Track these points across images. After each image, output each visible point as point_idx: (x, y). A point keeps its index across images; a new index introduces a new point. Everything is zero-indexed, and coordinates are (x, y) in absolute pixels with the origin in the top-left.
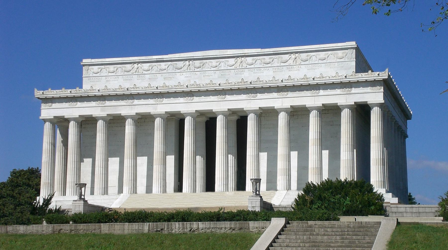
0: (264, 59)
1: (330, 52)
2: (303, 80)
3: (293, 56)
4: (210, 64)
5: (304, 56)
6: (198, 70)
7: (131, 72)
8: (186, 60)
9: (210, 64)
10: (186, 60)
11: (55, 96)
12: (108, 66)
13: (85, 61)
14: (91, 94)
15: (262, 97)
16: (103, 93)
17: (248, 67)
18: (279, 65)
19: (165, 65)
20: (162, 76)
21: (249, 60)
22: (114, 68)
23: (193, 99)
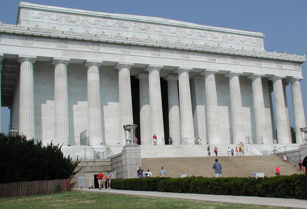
0: (200, 33)
3: (222, 35)
5: (229, 36)
6: (144, 32)
7: (77, 23)
8: (133, 21)
9: (155, 29)
10: (133, 21)
11: (8, 31)
12: (51, 13)
13: (22, 4)
14: (53, 35)
16: (68, 36)
18: (211, 40)
21: (188, 31)
22: (58, 16)
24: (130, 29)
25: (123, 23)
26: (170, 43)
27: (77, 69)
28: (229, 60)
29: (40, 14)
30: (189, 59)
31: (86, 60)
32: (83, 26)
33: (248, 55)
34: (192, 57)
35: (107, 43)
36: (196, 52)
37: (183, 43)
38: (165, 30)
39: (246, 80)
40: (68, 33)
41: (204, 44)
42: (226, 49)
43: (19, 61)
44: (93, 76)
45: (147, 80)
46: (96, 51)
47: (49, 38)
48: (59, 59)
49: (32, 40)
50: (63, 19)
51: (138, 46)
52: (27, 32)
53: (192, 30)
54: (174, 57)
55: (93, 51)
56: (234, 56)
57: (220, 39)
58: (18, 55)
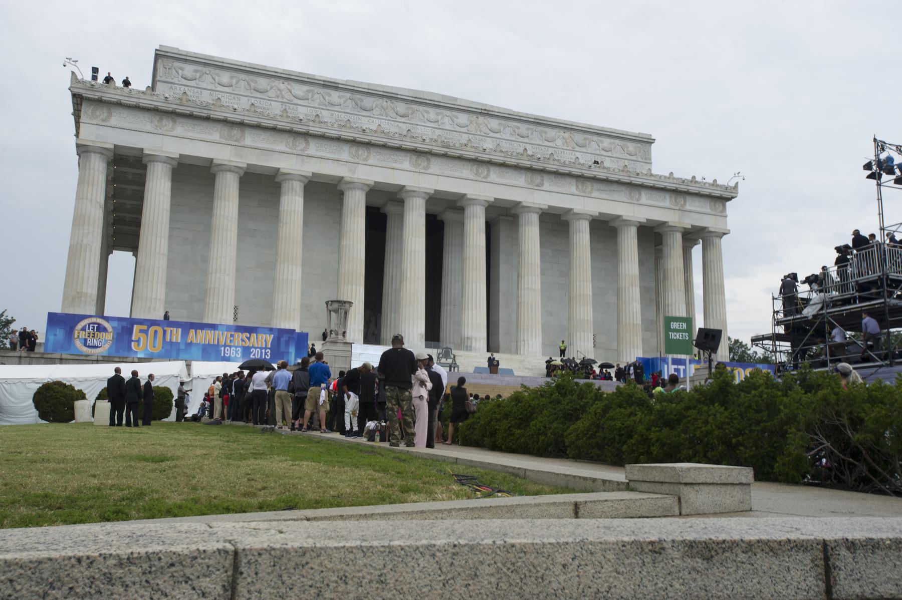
0: (518, 128)
1: (617, 142)
2: (621, 173)
4: (426, 115)
6: (403, 120)
7: (270, 94)
8: (383, 96)
9: (426, 115)
12: (217, 71)
14: (215, 114)
15: (551, 188)
16: (246, 118)
17: (491, 134)
18: (541, 143)
19: (339, 97)
20: (332, 115)
23: (427, 167)
24: (376, 112)
25: (362, 100)
26: (451, 144)
27: (261, 186)
28: (572, 187)
29: (196, 71)
30: (489, 180)
31: (279, 169)
32: (280, 100)
33: (612, 177)
34: (495, 175)
35: (323, 137)
36: (503, 165)
37: (476, 148)
38: (446, 120)
39: (605, 229)
40: (247, 113)
41: (521, 151)
42: (567, 163)
43: (145, 160)
44: (293, 203)
45: (401, 217)
46: (301, 153)
47: (208, 119)
48: (222, 163)
49: (175, 122)
50: (242, 83)
51: (384, 146)
52: (162, 105)
53: (503, 122)
54: (457, 174)
55: (295, 152)
56: (581, 178)
57: (559, 142)
58: (142, 150)
